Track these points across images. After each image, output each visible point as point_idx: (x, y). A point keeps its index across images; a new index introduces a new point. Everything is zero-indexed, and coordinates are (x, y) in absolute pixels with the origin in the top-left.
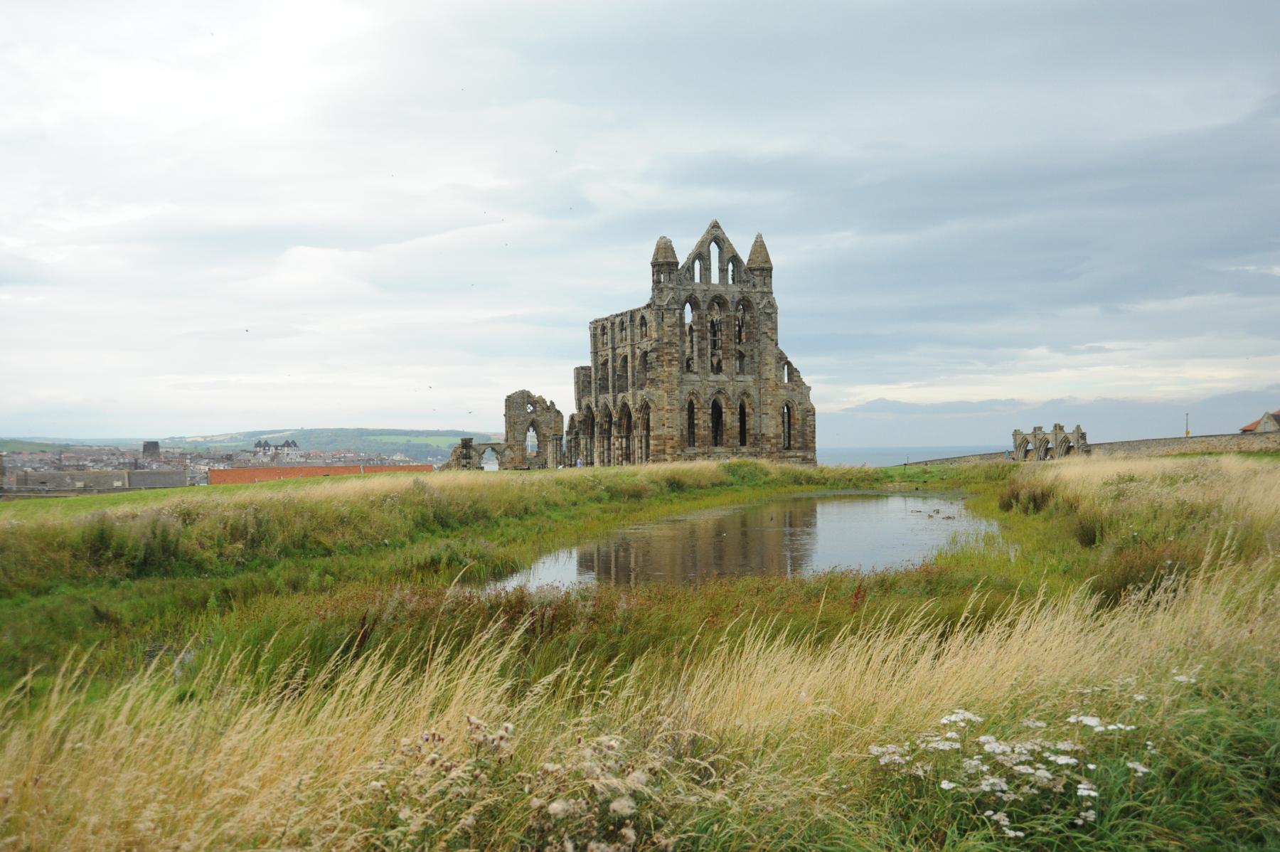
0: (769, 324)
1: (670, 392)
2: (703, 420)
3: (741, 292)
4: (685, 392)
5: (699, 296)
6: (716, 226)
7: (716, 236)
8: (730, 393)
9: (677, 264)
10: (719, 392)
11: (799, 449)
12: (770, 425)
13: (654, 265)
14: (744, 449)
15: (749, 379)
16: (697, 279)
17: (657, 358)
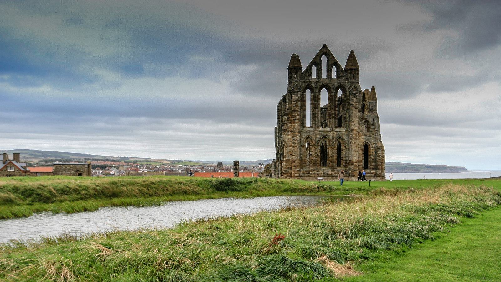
0: (355, 100)
1: (294, 137)
2: (316, 151)
3: (339, 83)
4: (304, 137)
5: (313, 85)
6: (325, 47)
7: (325, 51)
8: (331, 137)
9: (301, 68)
10: (324, 137)
11: (373, 169)
12: (356, 155)
13: (289, 69)
14: (339, 168)
15: (343, 130)
16: (314, 76)
17: (288, 119)
